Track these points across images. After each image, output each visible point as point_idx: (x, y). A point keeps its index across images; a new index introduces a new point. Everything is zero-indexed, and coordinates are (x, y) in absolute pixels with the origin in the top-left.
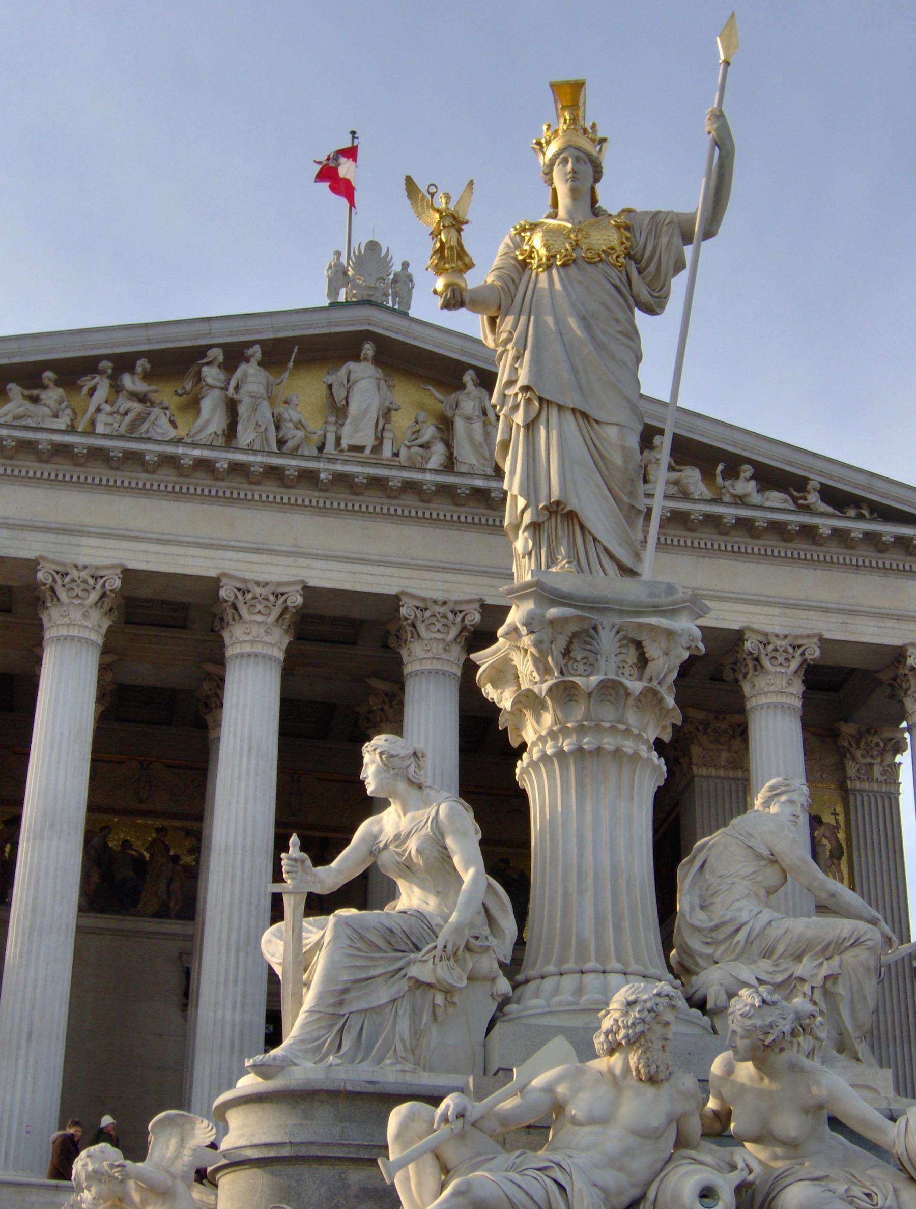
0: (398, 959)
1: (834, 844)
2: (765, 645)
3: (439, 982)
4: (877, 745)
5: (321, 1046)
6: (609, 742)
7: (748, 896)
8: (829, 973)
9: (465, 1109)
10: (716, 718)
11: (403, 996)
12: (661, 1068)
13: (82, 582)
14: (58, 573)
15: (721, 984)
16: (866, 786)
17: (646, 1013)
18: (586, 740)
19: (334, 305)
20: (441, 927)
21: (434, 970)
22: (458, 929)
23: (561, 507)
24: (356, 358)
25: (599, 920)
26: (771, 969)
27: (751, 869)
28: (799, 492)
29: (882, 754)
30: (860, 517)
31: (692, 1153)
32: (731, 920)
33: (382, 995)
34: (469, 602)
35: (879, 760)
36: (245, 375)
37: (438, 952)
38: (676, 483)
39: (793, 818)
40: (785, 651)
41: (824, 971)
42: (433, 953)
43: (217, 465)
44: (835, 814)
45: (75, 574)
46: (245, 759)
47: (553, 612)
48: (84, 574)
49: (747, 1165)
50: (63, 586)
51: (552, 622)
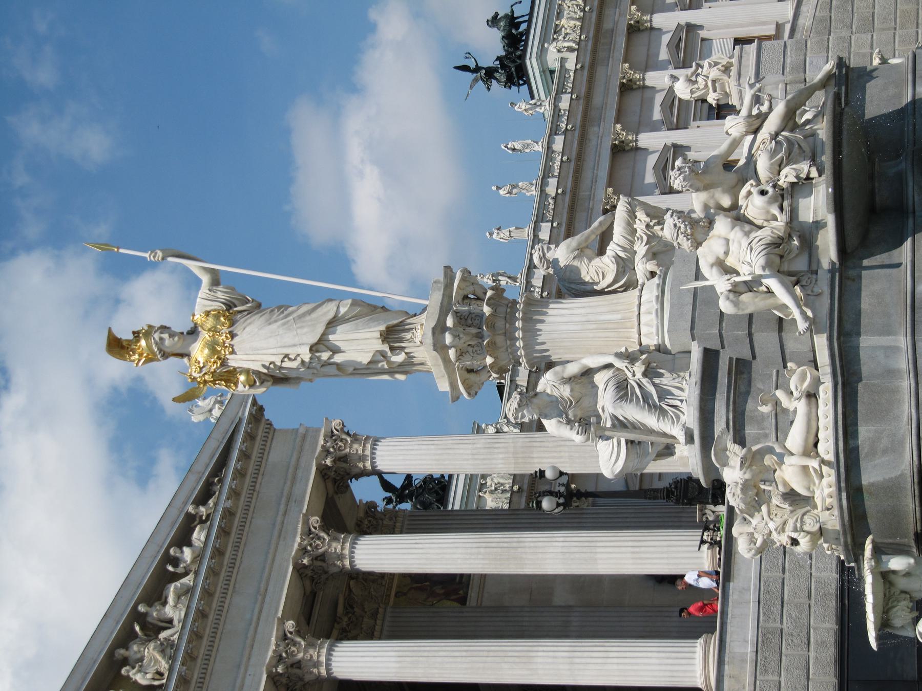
10: (338, 623)
26: (640, 241)
28: (195, 520)
29: (376, 519)
30: (221, 481)
33: (652, 389)
35: (380, 522)
37: (629, 366)
38: (178, 597)
40: (312, 539)
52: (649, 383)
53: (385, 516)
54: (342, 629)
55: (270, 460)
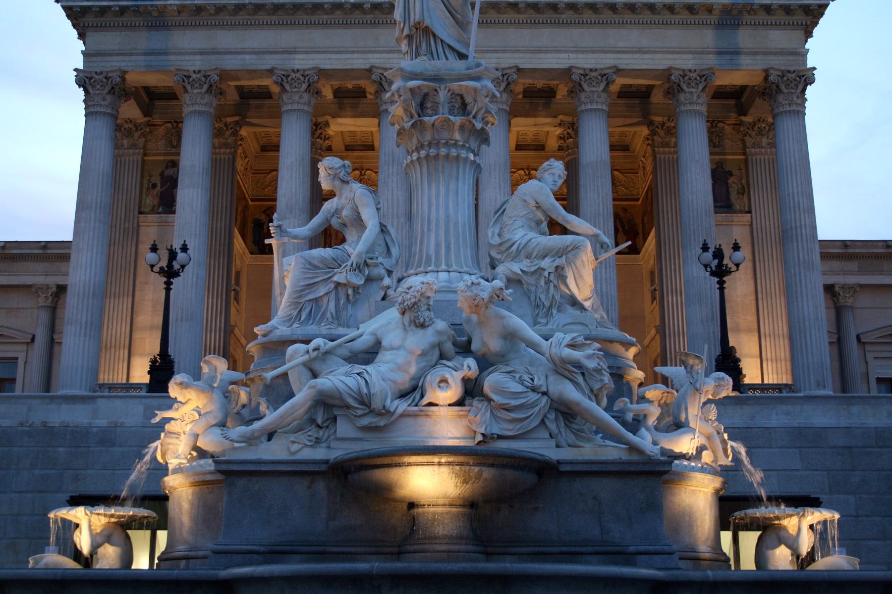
0: (329, 272)
1: (740, 186)
2: (683, 77)
3: (348, 282)
4: (765, 128)
5: (291, 318)
6: (443, 151)
7: (522, 226)
8: (558, 264)
9: (319, 346)
10: (668, 120)
11: (332, 291)
12: (427, 320)
13: (297, 79)
14: (284, 75)
15: (504, 274)
16: (758, 150)
17: (416, 292)
18: (431, 150)
20: (352, 254)
21: (346, 276)
22: (359, 255)
23: (421, 24)
25: (438, 246)
27: (526, 212)
31: (445, 362)
32: (509, 240)
33: (322, 291)
34: (510, 68)
37: (348, 267)
39: (553, 183)
40: (696, 79)
42: (346, 268)
43: (365, 6)
44: (740, 169)
45: (293, 75)
46: (391, 167)
48: (298, 75)
49: (468, 367)
50: (288, 82)
51: (412, 90)
52: (329, 289)
53: (771, 139)
54: (664, 124)
55: (772, 32)
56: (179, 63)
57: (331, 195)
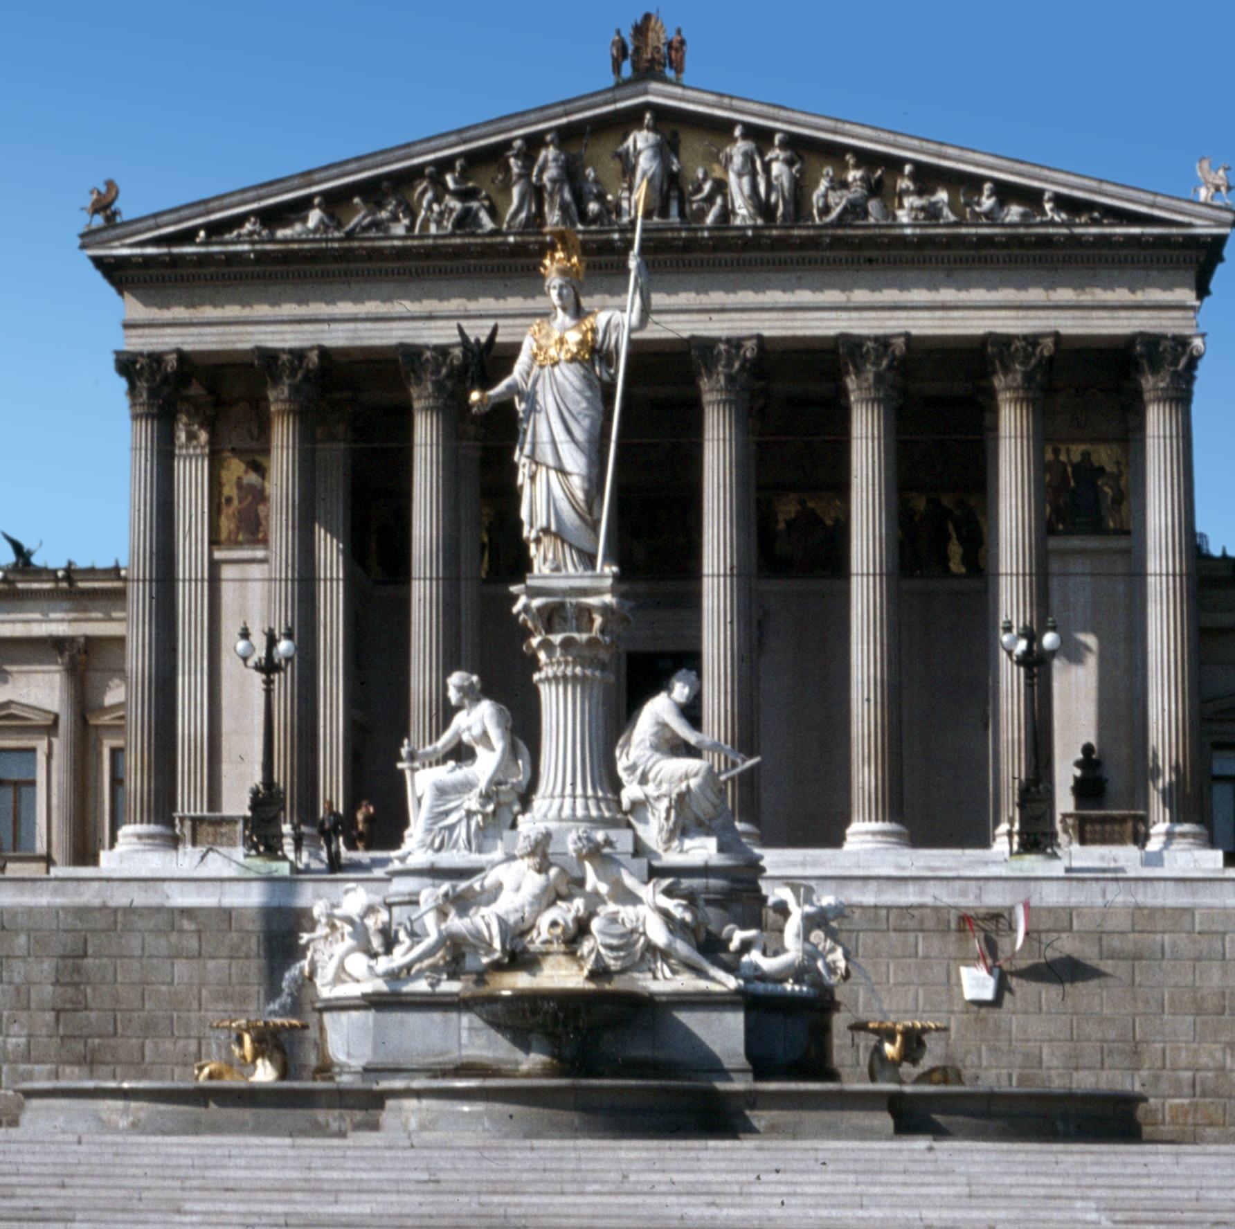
19: (618, 86)
24: (640, 128)
36: (546, 161)
38: (922, 209)
41: (676, 791)
47: (537, 603)
56: (261, 337)
57: (459, 708)
